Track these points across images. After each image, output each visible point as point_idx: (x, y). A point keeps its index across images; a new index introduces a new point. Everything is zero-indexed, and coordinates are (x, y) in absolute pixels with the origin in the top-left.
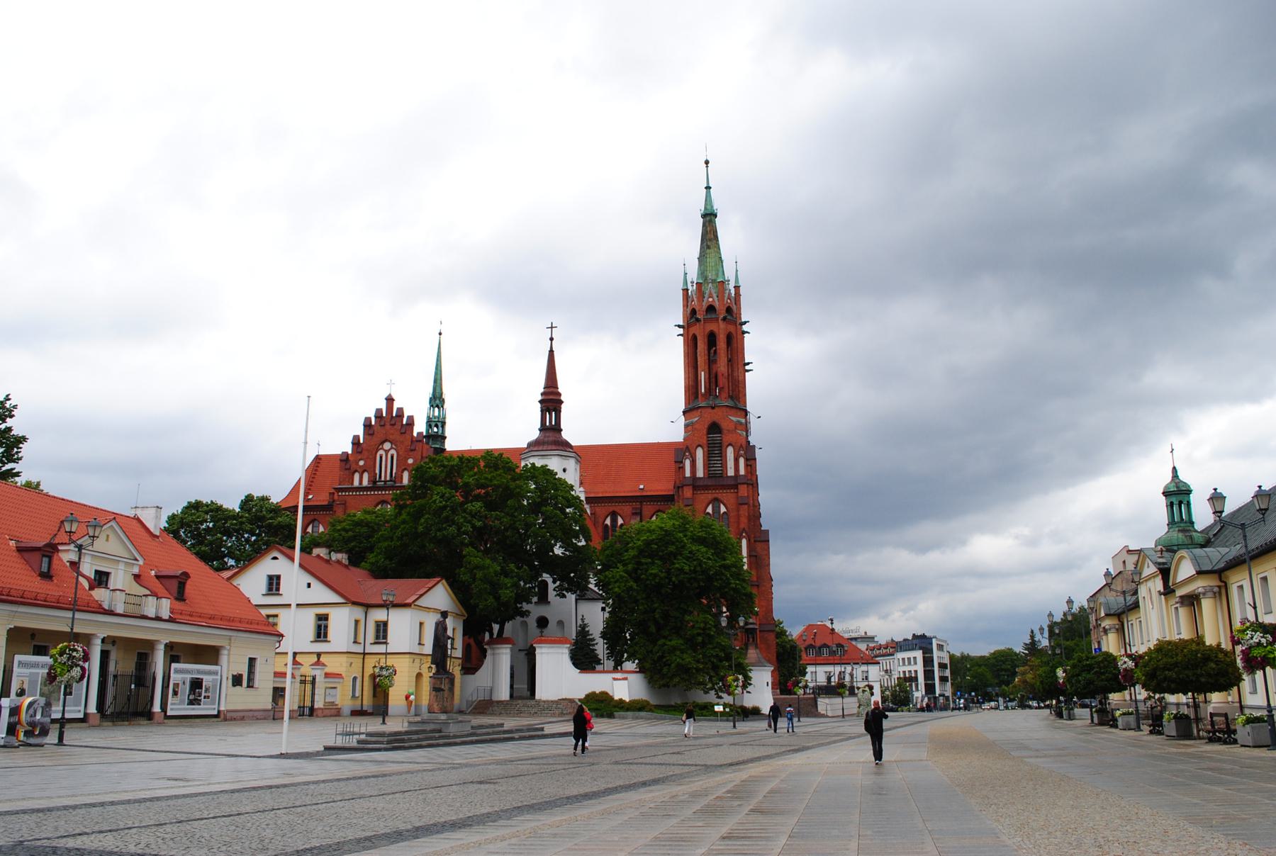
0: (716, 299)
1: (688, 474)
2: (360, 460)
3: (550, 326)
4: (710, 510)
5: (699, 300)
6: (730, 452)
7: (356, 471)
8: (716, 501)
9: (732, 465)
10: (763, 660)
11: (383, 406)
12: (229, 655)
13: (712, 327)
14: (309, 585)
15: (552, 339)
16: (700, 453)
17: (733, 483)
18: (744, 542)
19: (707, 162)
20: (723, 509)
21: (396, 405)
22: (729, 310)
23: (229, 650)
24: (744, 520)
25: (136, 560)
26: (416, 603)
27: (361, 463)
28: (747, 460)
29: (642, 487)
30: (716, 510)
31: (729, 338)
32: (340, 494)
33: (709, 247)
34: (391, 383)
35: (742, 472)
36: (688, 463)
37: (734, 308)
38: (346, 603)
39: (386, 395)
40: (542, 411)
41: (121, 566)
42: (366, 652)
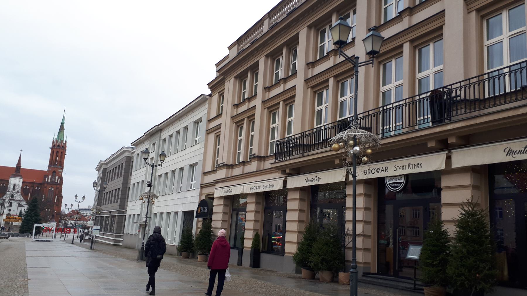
0: (60, 144)
1: (46, 181)
4: (50, 189)
5: (56, 143)
6: (57, 177)
8: (52, 187)
9: (57, 180)
10: (55, 221)
13: (58, 150)
15: (21, 153)
16: (50, 177)
17: (56, 184)
18: (56, 197)
19: (64, 111)
20: (53, 189)
22: (63, 146)
24: (57, 192)
28: (60, 180)
29: (35, 180)
30: (51, 189)
31: (62, 152)
33: (61, 131)
35: (59, 182)
36: (47, 179)
37: (64, 146)
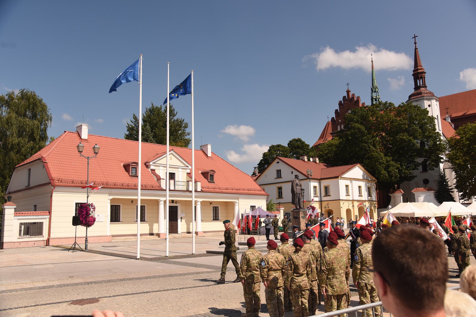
2: (339, 120)
3: (414, 37)
7: (338, 125)
11: (345, 94)
12: (239, 205)
14: (292, 173)
15: (415, 43)
21: (351, 94)
23: (238, 203)
25: (188, 167)
26: (343, 176)
27: (340, 121)
32: (333, 135)
34: (348, 84)
38: (308, 179)
39: (346, 90)
40: (414, 79)
41: (180, 170)
42: (322, 200)
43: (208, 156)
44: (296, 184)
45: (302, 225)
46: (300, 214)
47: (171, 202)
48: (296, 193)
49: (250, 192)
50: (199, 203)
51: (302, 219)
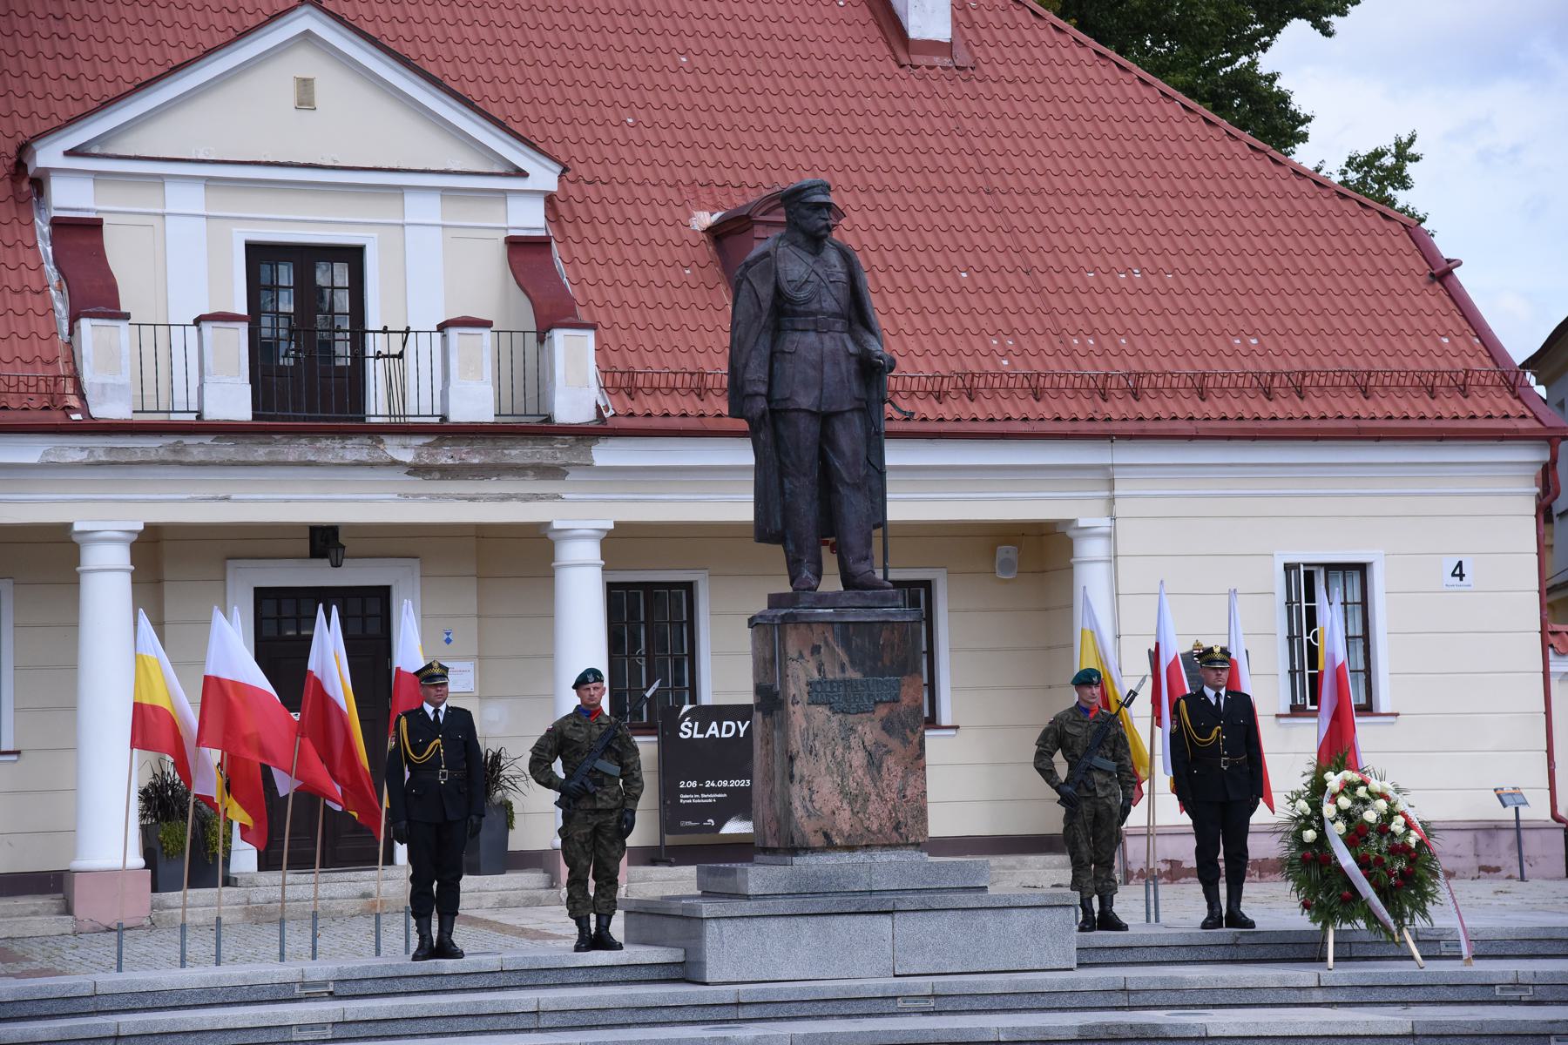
12: (1113, 559)
23: (1111, 536)
25: (521, 173)
41: (423, 209)
43: (913, 34)
44: (766, 305)
45: (826, 788)
46: (792, 652)
47: (307, 551)
48: (761, 404)
49: (1283, 407)
50: (589, 551)
51: (820, 709)
